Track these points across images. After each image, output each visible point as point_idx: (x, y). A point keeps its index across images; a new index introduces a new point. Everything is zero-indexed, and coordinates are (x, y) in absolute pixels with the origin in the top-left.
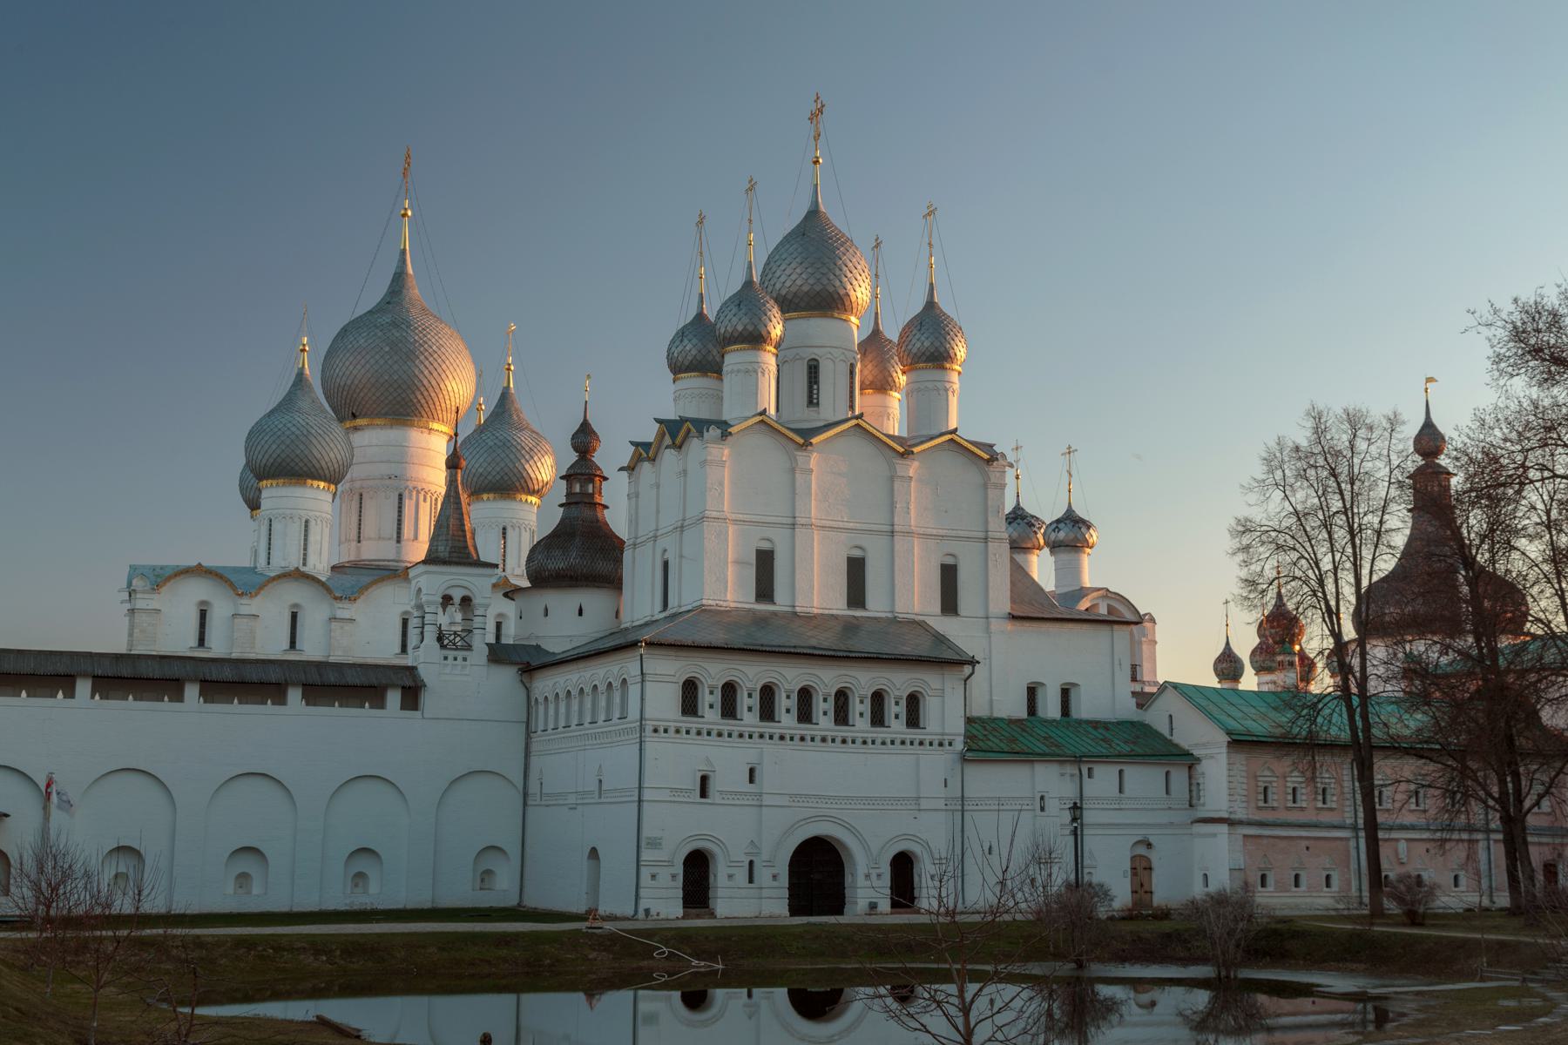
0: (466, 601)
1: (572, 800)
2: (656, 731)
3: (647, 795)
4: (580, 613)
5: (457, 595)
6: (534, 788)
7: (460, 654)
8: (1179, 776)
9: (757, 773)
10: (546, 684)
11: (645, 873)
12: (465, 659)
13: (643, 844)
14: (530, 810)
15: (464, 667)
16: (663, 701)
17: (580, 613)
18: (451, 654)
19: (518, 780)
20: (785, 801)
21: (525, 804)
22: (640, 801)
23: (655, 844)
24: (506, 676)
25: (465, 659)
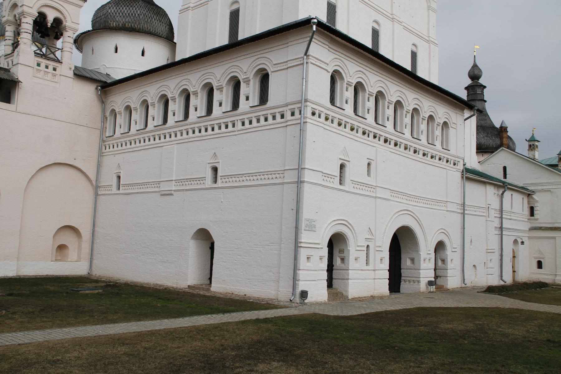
0: (58, 22)
1: (165, 187)
2: (313, 114)
3: (308, 176)
4: (143, 54)
5: (51, 16)
6: (109, 179)
7: (52, 64)
8: (526, 199)
9: (372, 167)
10: (118, 100)
11: (303, 253)
12: (55, 69)
13: (303, 225)
14: (101, 199)
15: (54, 75)
16: (318, 88)
17: (143, 54)
18: (44, 62)
19: (93, 177)
20: (386, 195)
21: (96, 195)
22: (300, 183)
23: (311, 228)
24: (88, 91)
25: (55, 69)
